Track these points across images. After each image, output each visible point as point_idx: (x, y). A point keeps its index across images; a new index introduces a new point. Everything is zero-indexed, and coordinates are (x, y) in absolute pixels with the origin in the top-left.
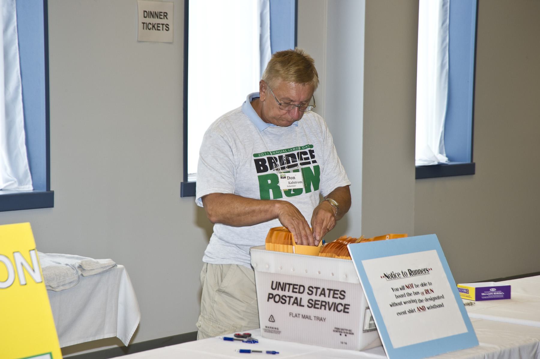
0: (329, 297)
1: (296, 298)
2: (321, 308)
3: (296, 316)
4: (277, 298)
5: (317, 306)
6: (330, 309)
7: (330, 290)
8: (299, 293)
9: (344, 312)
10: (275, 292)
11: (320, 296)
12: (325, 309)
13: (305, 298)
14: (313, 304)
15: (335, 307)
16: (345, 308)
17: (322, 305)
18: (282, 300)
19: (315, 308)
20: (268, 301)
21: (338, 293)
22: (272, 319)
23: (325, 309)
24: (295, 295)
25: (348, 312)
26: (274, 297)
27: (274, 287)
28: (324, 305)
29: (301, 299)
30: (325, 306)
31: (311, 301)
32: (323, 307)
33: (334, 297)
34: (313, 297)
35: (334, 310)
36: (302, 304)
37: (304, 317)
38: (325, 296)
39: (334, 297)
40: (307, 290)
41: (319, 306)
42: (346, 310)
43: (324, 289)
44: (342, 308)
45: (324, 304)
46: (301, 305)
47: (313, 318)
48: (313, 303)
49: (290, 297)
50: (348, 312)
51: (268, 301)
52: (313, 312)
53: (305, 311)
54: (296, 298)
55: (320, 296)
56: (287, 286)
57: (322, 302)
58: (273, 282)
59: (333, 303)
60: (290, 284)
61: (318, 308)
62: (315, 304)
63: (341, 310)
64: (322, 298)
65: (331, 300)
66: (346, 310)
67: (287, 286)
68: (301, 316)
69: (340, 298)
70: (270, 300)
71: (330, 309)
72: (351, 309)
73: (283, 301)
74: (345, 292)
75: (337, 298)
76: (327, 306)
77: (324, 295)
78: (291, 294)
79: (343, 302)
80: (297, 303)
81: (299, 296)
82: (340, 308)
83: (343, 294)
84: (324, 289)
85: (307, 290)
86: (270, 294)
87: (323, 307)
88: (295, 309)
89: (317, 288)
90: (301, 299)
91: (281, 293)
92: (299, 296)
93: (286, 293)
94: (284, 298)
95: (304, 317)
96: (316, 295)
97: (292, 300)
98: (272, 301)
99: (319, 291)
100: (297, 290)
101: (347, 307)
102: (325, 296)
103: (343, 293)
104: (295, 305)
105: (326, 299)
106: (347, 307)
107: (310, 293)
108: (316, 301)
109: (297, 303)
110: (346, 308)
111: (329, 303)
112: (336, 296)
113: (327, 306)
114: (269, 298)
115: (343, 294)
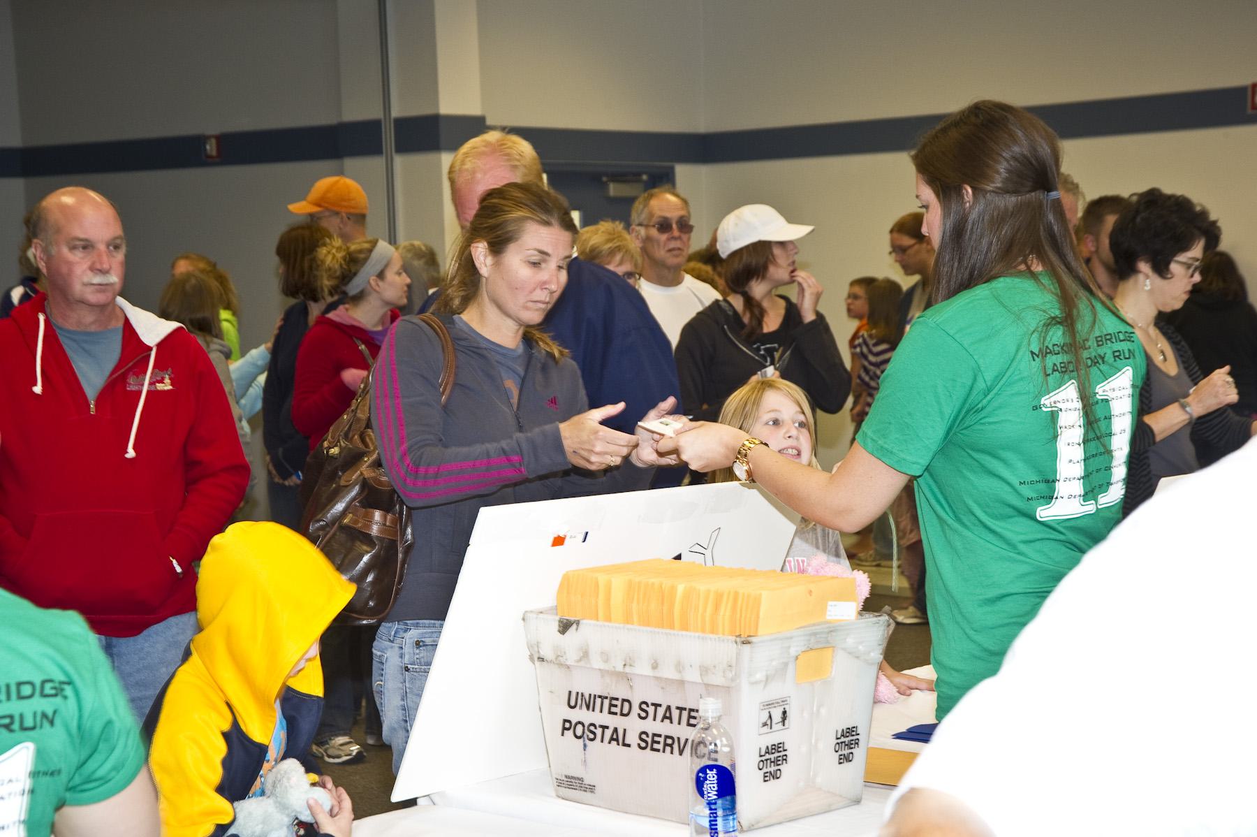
8: (622, 714)
14: (649, 742)
17: (666, 745)
19: (653, 749)
30: (671, 746)
32: (668, 749)
34: (652, 726)
41: (660, 747)
45: (669, 741)
46: (625, 745)
48: (649, 740)
57: (667, 737)
71: (681, 753)
76: (676, 746)
100: (617, 710)
109: (617, 740)
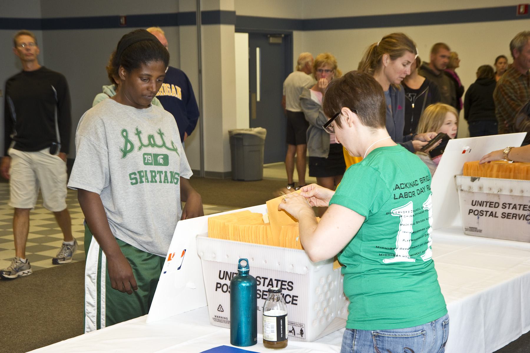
6: (520, 219)
8: (495, 207)
10: (474, 208)
13: (500, 211)
14: (505, 216)
19: (507, 218)
27: (474, 204)
28: (515, 216)
29: (496, 213)
30: (516, 217)
32: (514, 218)
33: (523, 210)
34: (507, 211)
36: (497, 216)
40: (501, 206)
41: (511, 217)
46: (495, 217)
48: (506, 215)
49: (487, 212)
54: (492, 212)
56: (485, 203)
57: (514, 214)
60: (487, 202)
62: (508, 216)
67: (485, 203)
71: (520, 219)
76: (517, 217)
77: (516, 208)
80: (492, 215)
81: (494, 210)
84: (515, 205)
86: (470, 210)
87: (514, 218)
89: (510, 204)
90: (496, 213)
91: (479, 208)
97: (488, 214)
98: (472, 214)
99: (511, 206)
100: (493, 206)
104: (491, 217)
108: (508, 214)
109: (492, 215)
114: (470, 212)
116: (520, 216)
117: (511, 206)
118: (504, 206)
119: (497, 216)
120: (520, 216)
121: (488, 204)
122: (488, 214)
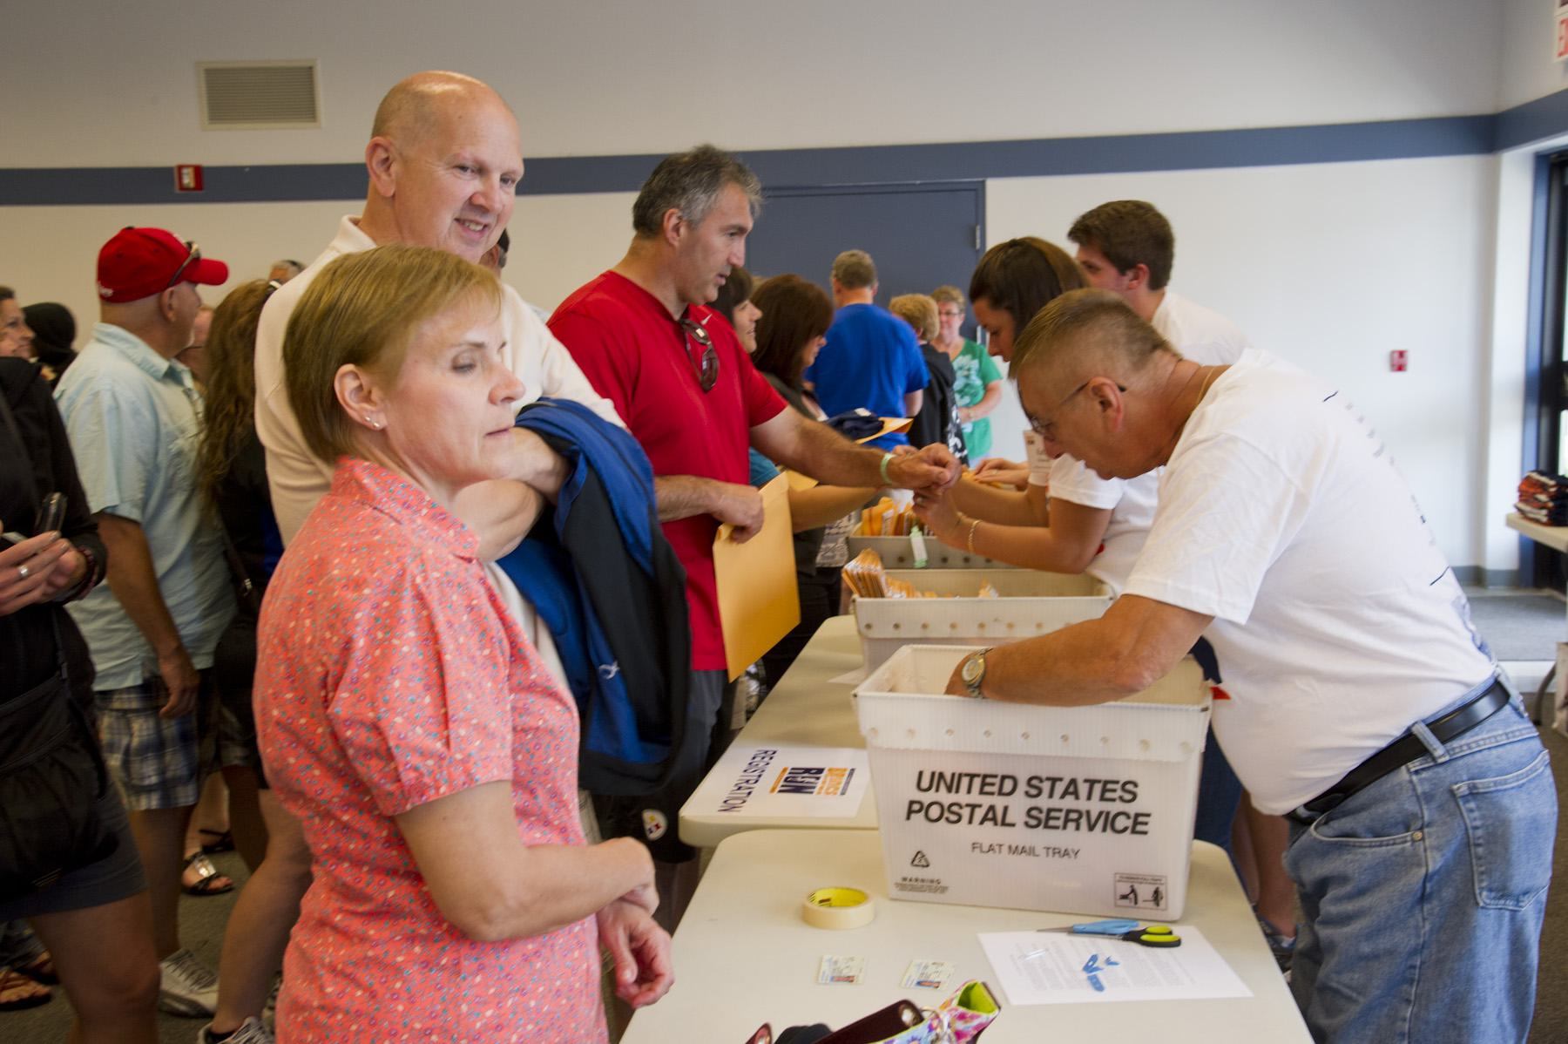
0: (1089, 798)
1: (992, 808)
2: (1065, 827)
3: (991, 848)
4: (935, 812)
5: (1052, 823)
6: (1091, 828)
7: (1092, 782)
8: (1001, 793)
9: (1134, 832)
11: (1062, 797)
12: (1078, 828)
13: (1018, 805)
14: (1040, 820)
15: (1109, 822)
16: (1136, 823)
17: (1067, 820)
18: (950, 814)
19: (1047, 826)
20: (908, 818)
21: (1118, 787)
22: (920, 859)
23: (1078, 828)
24: (986, 801)
25: (1145, 833)
26: (925, 809)
27: (925, 784)
28: (1073, 819)
29: (1006, 809)
30: (1077, 821)
31: (1034, 813)
32: (1071, 825)
33: (1102, 798)
34: (1044, 802)
35: (1104, 830)
36: (1008, 820)
37: (1014, 850)
38: (1077, 798)
39: (1102, 798)
40: (1022, 787)
41: (1060, 823)
42: (1139, 828)
43: (1073, 782)
44: (1129, 823)
45: (1074, 816)
46: (1004, 824)
47: (1040, 850)
48: (1043, 816)
49: (973, 807)
50: (1145, 833)
51: (908, 818)
52: (1041, 837)
53: (1019, 835)
54: (992, 808)
55: (1062, 797)
56: (965, 781)
57: (1069, 812)
58: (921, 774)
59: (1101, 814)
60: (972, 776)
61: (1056, 828)
62: (1048, 818)
63: (1125, 829)
64: (1069, 802)
65: (1095, 806)
66: (1139, 828)
67: (965, 781)
68: (1005, 849)
69: (1121, 798)
70: (913, 816)
71: (1091, 828)
72: (1153, 825)
73: (954, 818)
74: (1136, 785)
75: (1113, 800)
76: (1083, 821)
78: (975, 798)
79: (1132, 809)
80: (994, 819)
81: (999, 802)
82: (1121, 822)
83: (1129, 790)
84: (1073, 782)
85: (1022, 787)
86: (912, 803)
87: (1071, 825)
88: (990, 833)
89: (1054, 781)
90: (1006, 809)
91: (945, 797)
92: (999, 802)
93: (962, 797)
94: (955, 808)
95: (1014, 850)
96: (1051, 796)
97: (979, 814)
98: (918, 818)
99: (1060, 787)
100: (995, 789)
101: (1141, 819)
102: (1077, 798)
103: (1129, 787)
104: (989, 824)
105: (1082, 804)
106: (1141, 819)
107: (1034, 792)
108: (1050, 810)
109: (994, 819)
110: (1138, 824)
111: (1088, 813)
112: (1108, 795)
113: (1083, 821)
114: (910, 812)
115: (1129, 790)
116: (1094, 817)
117: (1060, 787)
118: (1034, 785)
119: (1008, 820)
120: (1094, 817)
121: (977, 782)
122: (979, 814)
